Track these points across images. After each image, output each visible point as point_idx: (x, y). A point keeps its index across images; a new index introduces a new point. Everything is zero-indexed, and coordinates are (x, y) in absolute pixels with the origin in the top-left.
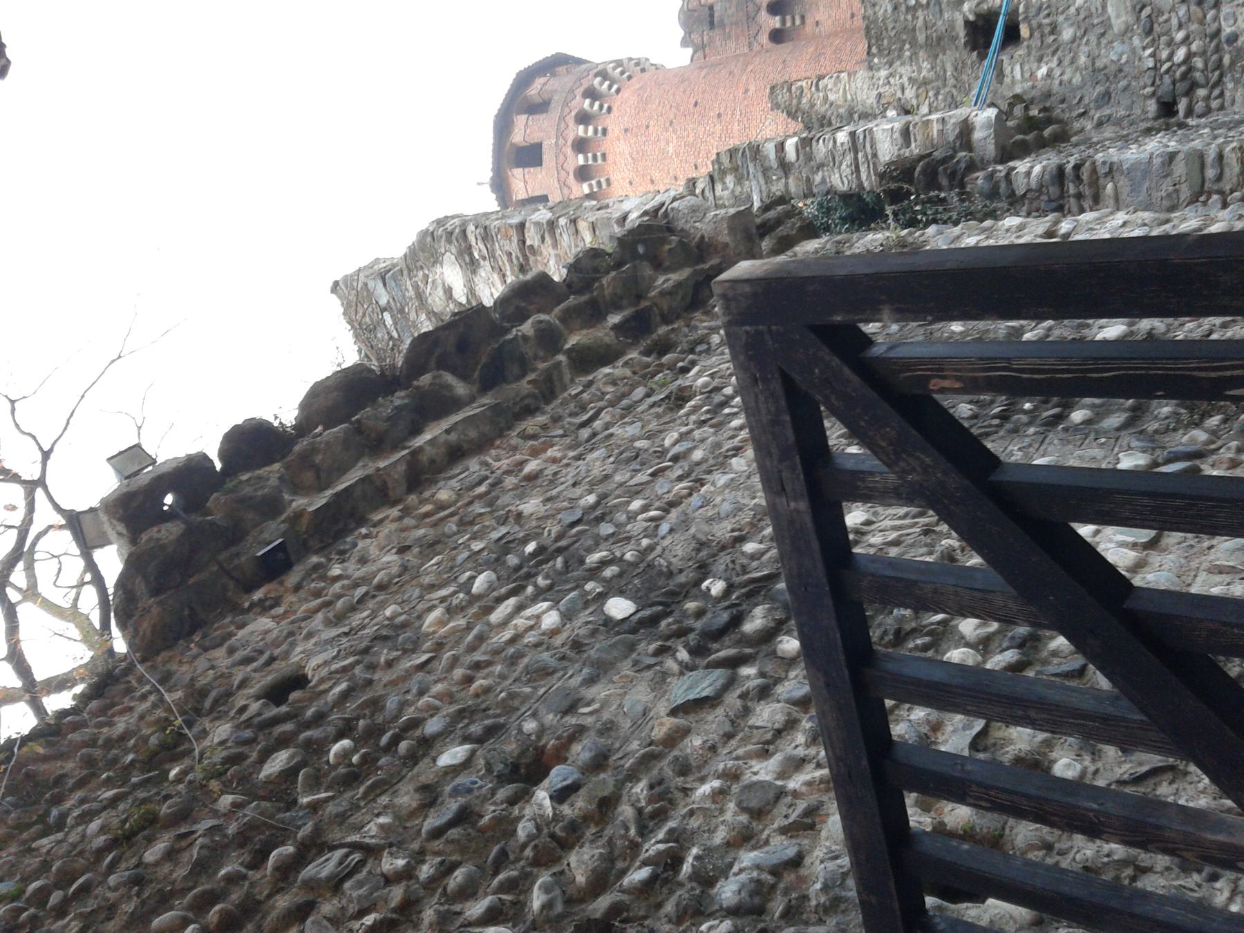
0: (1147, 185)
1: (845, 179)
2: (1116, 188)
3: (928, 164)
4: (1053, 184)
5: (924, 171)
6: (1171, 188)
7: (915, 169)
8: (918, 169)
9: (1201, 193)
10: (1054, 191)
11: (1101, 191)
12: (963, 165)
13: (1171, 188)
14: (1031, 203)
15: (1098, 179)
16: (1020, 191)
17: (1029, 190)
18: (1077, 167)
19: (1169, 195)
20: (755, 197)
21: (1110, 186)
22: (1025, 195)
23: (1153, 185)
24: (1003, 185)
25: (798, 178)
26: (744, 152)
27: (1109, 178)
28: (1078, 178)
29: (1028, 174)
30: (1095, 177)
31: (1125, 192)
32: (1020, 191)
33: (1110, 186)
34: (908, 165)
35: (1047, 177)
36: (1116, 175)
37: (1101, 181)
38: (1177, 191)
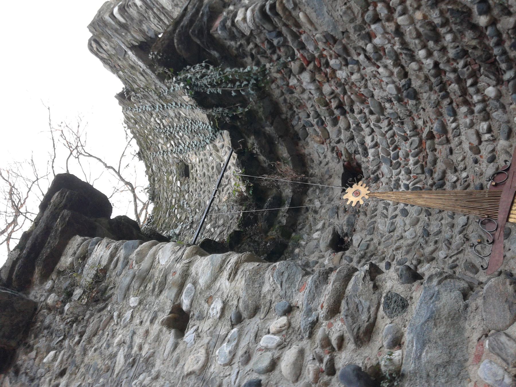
0: (325, 9)
1: (158, 26)
2: (306, 16)
3: (179, 34)
4: (264, 23)
5: (180, 41)
6: (344, 7)
7: (174, 43)
8: (175, 41)
9: (368, 5)
10: (267, 26)
11: (297, 20)
12: (205, 19)
13: (344, 7)
14: (259, 37)
15: (290, 13)
16: (247, 33)
17: (252, 31)
18: (273, 7)
19: (345, 13)
20: (123, 47)
21: (301, 15)
22: (251, 33)
23: (330, 8)
24: (234, 30)
25: (135, 31)
26: (98, 24)
27: (298, 10)
28: (277, 14)
29: (244, 19)
30: (287, 13)
31: (313, 16)
32: (247, 33)
33: (301, 15)
34: (167, 42)
35: (257, 20)
36: (301, 6)
37: (294, 13)
38: (349, 8)
